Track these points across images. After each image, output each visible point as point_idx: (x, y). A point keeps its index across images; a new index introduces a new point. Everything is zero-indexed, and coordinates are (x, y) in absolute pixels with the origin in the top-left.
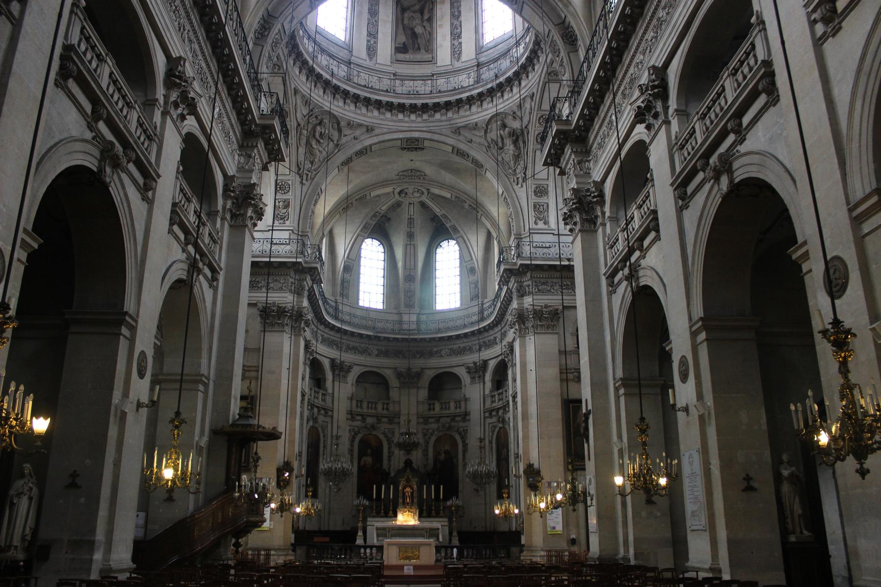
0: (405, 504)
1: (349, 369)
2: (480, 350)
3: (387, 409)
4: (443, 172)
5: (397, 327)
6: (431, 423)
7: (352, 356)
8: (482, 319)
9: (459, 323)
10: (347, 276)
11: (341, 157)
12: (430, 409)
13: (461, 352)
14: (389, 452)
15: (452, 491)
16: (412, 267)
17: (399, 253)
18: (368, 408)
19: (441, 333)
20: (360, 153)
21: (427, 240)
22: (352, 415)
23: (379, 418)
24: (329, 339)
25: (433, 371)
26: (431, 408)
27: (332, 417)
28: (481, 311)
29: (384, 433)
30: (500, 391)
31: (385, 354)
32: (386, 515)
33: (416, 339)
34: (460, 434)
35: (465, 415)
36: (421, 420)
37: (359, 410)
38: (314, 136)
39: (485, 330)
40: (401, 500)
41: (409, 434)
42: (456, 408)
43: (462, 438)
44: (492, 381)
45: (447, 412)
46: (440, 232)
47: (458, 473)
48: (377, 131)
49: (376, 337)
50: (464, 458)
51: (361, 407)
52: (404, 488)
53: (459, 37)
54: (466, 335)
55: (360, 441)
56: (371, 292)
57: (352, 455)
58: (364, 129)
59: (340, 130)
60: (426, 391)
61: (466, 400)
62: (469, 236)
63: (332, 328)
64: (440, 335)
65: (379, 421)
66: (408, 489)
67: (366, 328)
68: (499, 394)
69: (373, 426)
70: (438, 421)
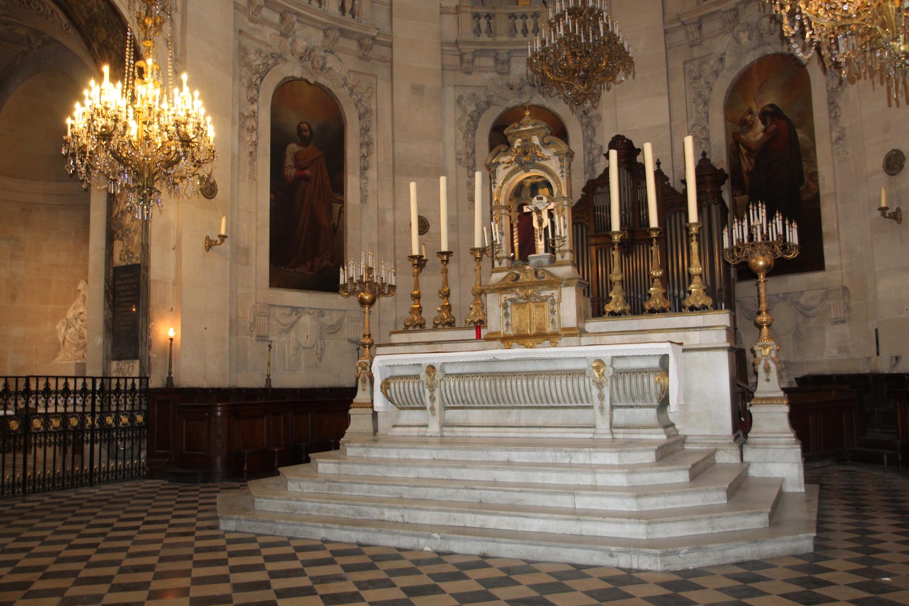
18: (513, 31)
22: (460, 58)
51: (490, 31)
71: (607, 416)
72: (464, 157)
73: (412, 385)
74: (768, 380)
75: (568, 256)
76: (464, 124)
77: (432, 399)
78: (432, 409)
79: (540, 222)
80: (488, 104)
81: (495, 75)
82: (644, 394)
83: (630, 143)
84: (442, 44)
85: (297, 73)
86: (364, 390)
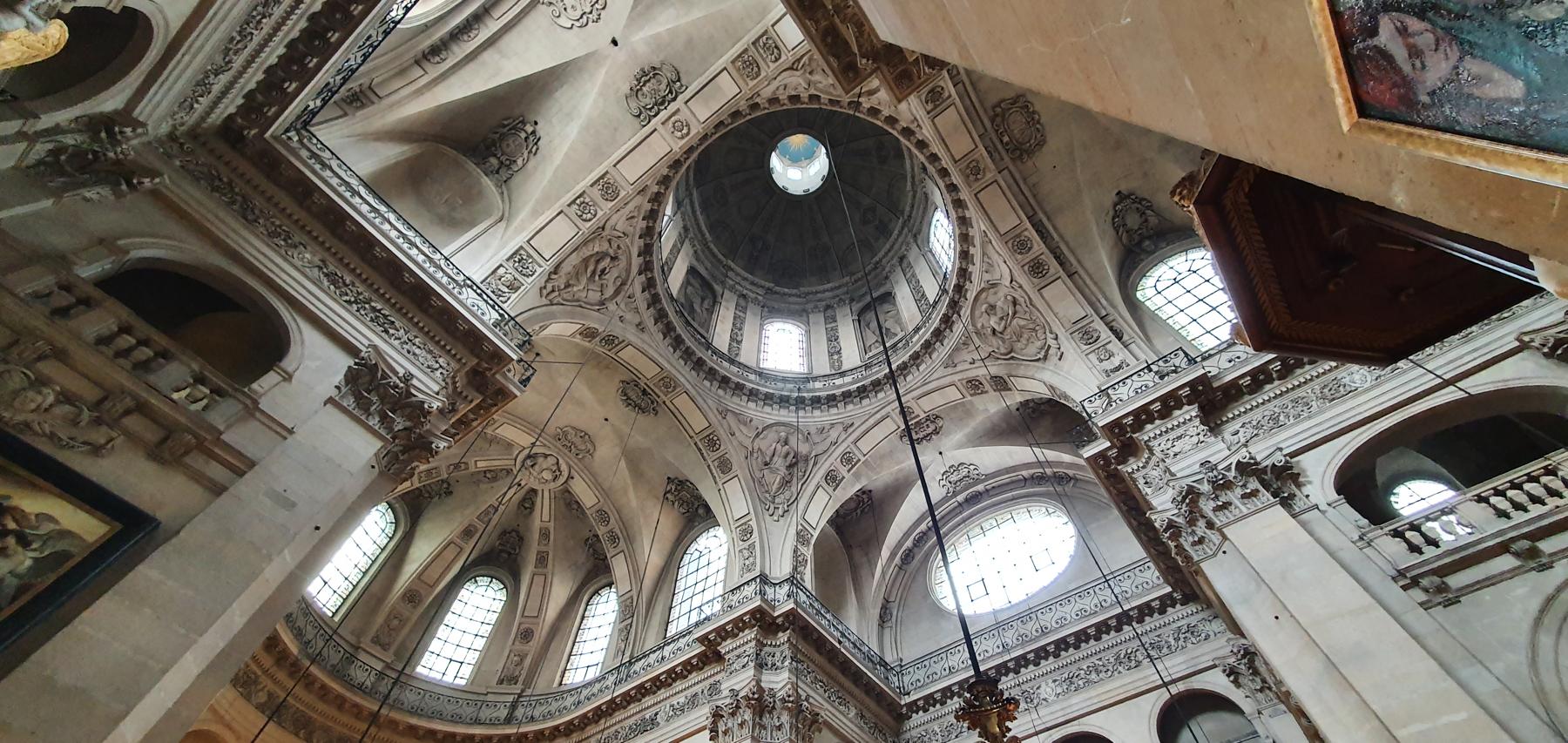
4: (623, 464)
8: (509, 720)
9: (469, 711)
11: (595, 321)
17: (422, 551)
19: (420, 716)
20: (610, 340)
28: (514, 706)
38: (598, 262)
46: (500, 557)
48: (645, 337)
53: (739, 342)
56: (333, 583)
58: (637, 321)
59: (617, 292)
62: (556, 581)
64: (414, 721)
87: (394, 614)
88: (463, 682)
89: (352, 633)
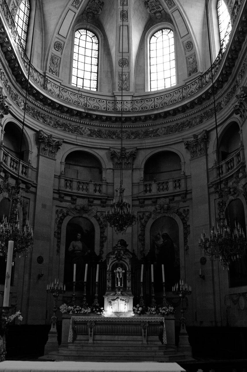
0: (113, 289)
1: (58, 146)
2: (201, 122)
3: (100, 191)
5: (110, 106)
6: (148, 205)
7: (61, 133)
9: (176, 96)
10: (58, 53)
12: (146, 191)
13: (180, 127)
14: (101, 237)
15: (174, 276)
16: (125, 50)
18: (78, 188)
19: (157, 109)
21: (141, 27)
23: (91, 199)
24: (33, 109)
25: (149, 151)
26: (147, 189)
27: (35, 194)
29: (96, 217)
30: (228, 160)
31: (99, 134)
32: (90, 304)
33: (130, 118)
34: (180, 215)
35: (187, 192)
36: (137, 203)
37: (68, 190)
39: (208, 95)
40: (109, 284)
41: (121, 205)
42: (175, 187)
43: (183, 219)
44: (218, 152)
45: (166, 192)
47: (179, 259)
49: (87, 114)
50: (186, 242)
51: (71, 187)
52: (115, 267)
54: (184, 108)
55: (69, 224)
57: (59, 238)
60: (142, 173)
61: (186, 177)
62: (185, 8)
63: (37, 95)
64: (156, 112)
65: (91, 203)
66: (119, 270)
67: (78, 104)
68: (227, 163)
69: (84, 210)
70: (155, 203)
71: (146, 338)
72: (56, 234)
73: (83, 327)
74: (183, 329)
75: (130, 289)
76: (58, 221)
77: (91, 332)
78: (91, 335)
79: (119, 276)
80: (67, 214)
81: (70, 204)
82: (99, 332)
83: (126, 242)
84: (54, 189)
85: (7, 196)
86: (54, 327)
87: (121, 75)
88: (175, 85)
89: (109, 92)
